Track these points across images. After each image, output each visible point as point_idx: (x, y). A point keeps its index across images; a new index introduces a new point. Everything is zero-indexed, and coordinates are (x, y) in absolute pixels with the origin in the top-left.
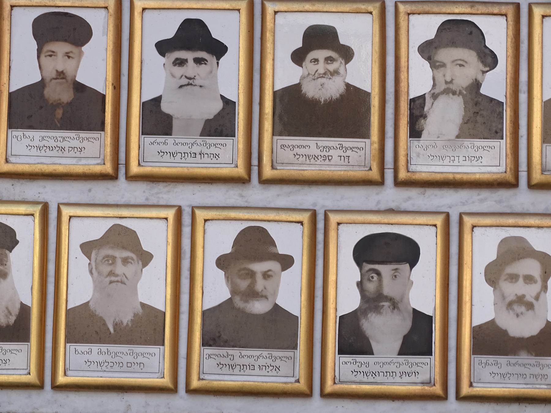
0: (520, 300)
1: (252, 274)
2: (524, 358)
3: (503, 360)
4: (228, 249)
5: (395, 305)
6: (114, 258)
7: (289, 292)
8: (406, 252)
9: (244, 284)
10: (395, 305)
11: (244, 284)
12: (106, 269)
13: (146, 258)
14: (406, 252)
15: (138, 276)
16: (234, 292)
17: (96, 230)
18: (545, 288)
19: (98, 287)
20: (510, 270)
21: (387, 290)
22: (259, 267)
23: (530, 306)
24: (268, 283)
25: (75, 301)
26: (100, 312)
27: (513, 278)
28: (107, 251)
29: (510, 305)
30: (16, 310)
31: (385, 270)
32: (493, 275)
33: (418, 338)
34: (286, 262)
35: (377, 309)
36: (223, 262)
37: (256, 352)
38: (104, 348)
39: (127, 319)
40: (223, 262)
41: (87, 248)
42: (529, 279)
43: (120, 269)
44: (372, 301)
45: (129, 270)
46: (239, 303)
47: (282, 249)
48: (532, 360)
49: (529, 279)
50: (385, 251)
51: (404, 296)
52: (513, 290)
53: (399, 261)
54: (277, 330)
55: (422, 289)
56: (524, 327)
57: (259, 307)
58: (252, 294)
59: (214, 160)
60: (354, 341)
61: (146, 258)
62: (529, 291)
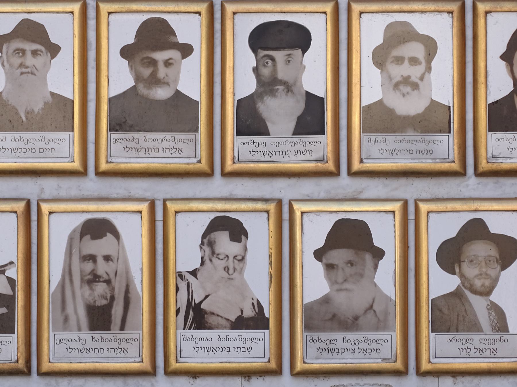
0: (406, 81)
1: (154, 63)
2: (411, 135)
3: (390, 137)
4: (131, 40)
5: (289, 88)
6: (23, 51)
7: (190, 79)
8: (299, 38)
9: (146, 72)
10: (289, 88)
11: (146, 72)
12: (17, 61)
13: (54, 50)
14: (299, 38)
15: (47, 66)
16: (138, 78)
18: (429, 69)
19: (10, 78)
20: (396, 53)
21: (281, 75)
22: (160, 56)
23: (415, 86)
24: (170, 71)
27: (399, 60)
28: (17, 44)
29: (397, 86)
31: (279, 55)
32: (380, 58)
33: (311, 119)
34: (186, 50)
35: (272, 93)
36: (127, 52)
37: (160, 136)
38: (17, 135)
39: (38, 107)
40: (127, 52)
42: (414, 61)
43: (30, 60)
44: (268, 85)
45: (38, 62)
46: (142, 90)
47: (181, 39)
48: (418, 137)
49: (414, 61)
50: (279, 39)
51: (297, 80)
52: (398, 72)
53: (292, 47)
54: (179, 113)
55: (314, 72)
56: (410, 106)
57: (162, 93)
58: (154, 81)
60: (251, 122)
62: (415, 72)
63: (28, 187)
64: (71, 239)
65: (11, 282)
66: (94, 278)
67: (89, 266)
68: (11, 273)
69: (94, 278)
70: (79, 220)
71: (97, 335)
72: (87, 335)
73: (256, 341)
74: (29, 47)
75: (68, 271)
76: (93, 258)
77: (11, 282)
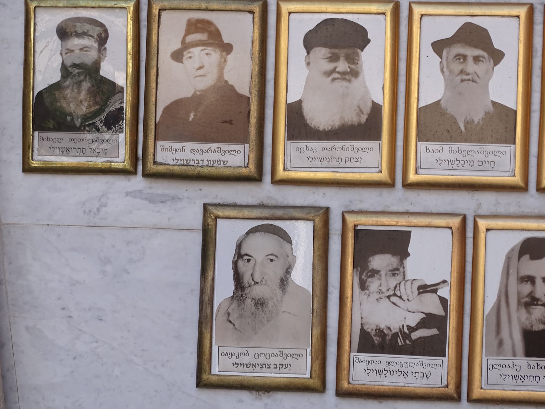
6: (465, 57)
12: (457, 67)
13: (497, 56)
15: (489, 74)
17: (448, 28)
19: (449, 85)
25: (427, 100)
26: (451, 110)
30: (367, 109)
38: (455, 146)
39: (478, 117)
41: (439, 47)
43: (471, 67)
45: (480, 69)
59: (355, 164)
61: (497, 56)
63: (464, 202)
64: (508, 259)
65: (444, 302)
66: (532, 301)
67: (527, 288)
68: (444, 292)
69: (532, 301)
70: (519, 238)
71: (533, 361)
72: (522, 361)
73: (435, 367)
74: (471, 52)
75: (504, 292)
76: (531, 279)
77: (444, 302)
